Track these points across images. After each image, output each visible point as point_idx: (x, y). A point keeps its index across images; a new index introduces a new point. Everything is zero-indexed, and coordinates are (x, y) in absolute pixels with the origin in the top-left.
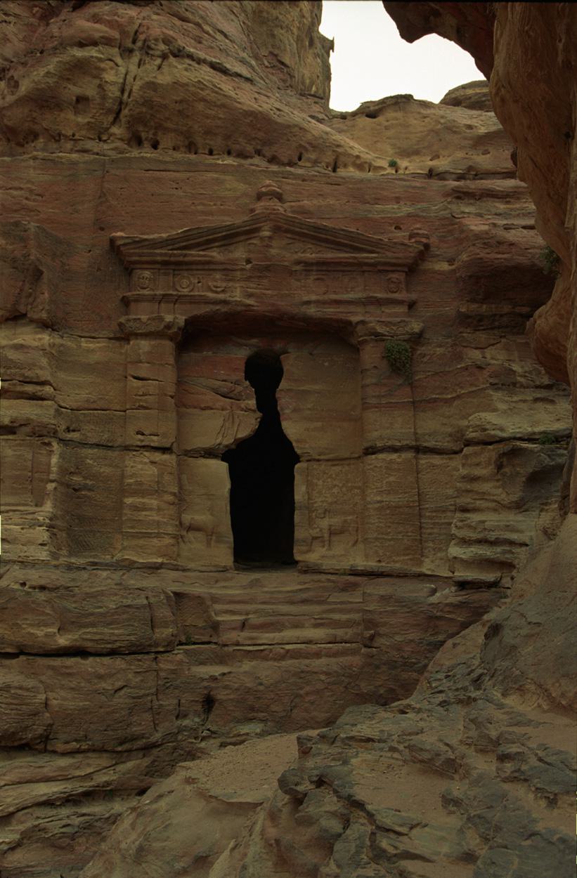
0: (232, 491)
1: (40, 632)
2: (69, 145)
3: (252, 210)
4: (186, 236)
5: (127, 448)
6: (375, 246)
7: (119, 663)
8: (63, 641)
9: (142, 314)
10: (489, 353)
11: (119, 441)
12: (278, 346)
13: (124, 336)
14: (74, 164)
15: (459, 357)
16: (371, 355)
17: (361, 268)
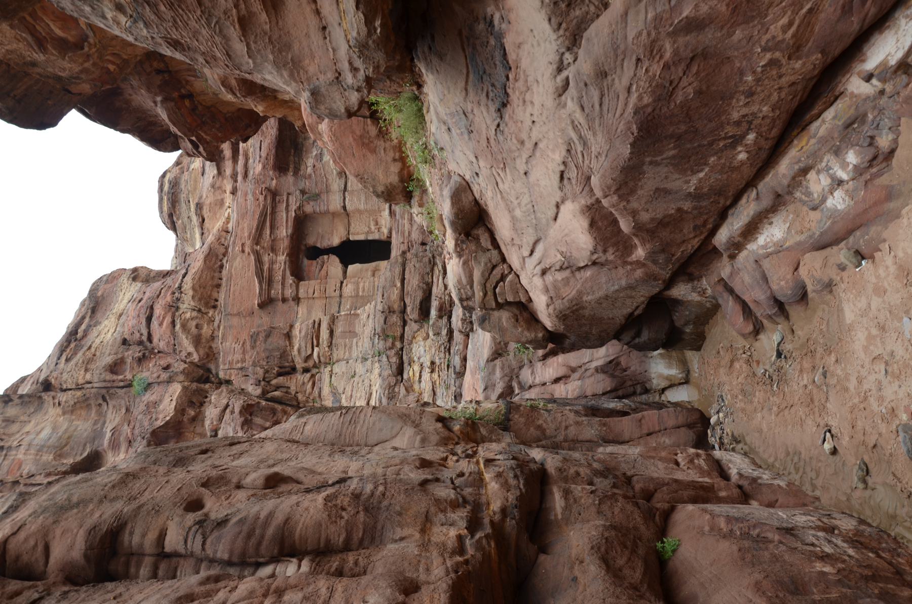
0: (360, 263)
1: (396, 292)
2: (216, 332)
3: (249, 254)
4: (258, 277)
5: (341, 296)
6: (264, 206)
7: (407, 269)
8: (399, 285)
9: (289, 292)
10: (309, 164)
11: (338, 299)
12: (303, 248)
13: (297, 299)
14: (225, 327)
15: (310, 175)
16: (308, 209)
17: (273, 213)
